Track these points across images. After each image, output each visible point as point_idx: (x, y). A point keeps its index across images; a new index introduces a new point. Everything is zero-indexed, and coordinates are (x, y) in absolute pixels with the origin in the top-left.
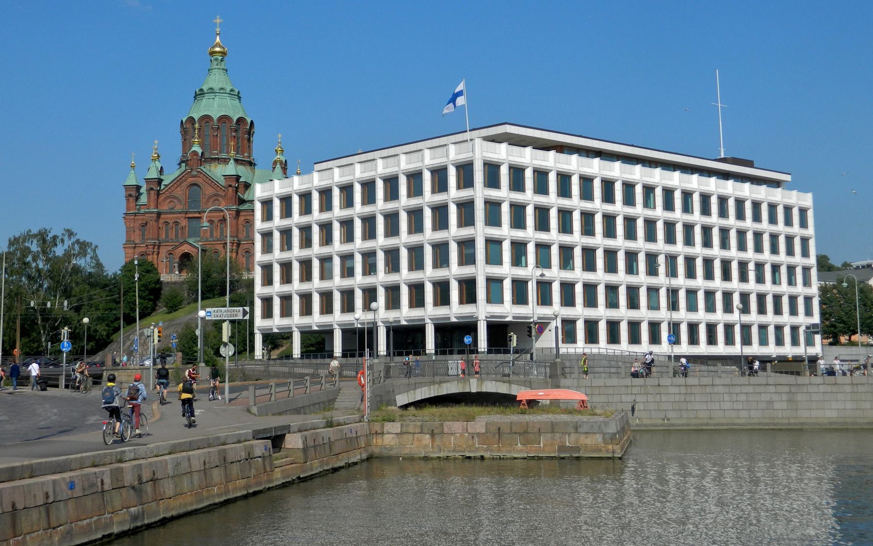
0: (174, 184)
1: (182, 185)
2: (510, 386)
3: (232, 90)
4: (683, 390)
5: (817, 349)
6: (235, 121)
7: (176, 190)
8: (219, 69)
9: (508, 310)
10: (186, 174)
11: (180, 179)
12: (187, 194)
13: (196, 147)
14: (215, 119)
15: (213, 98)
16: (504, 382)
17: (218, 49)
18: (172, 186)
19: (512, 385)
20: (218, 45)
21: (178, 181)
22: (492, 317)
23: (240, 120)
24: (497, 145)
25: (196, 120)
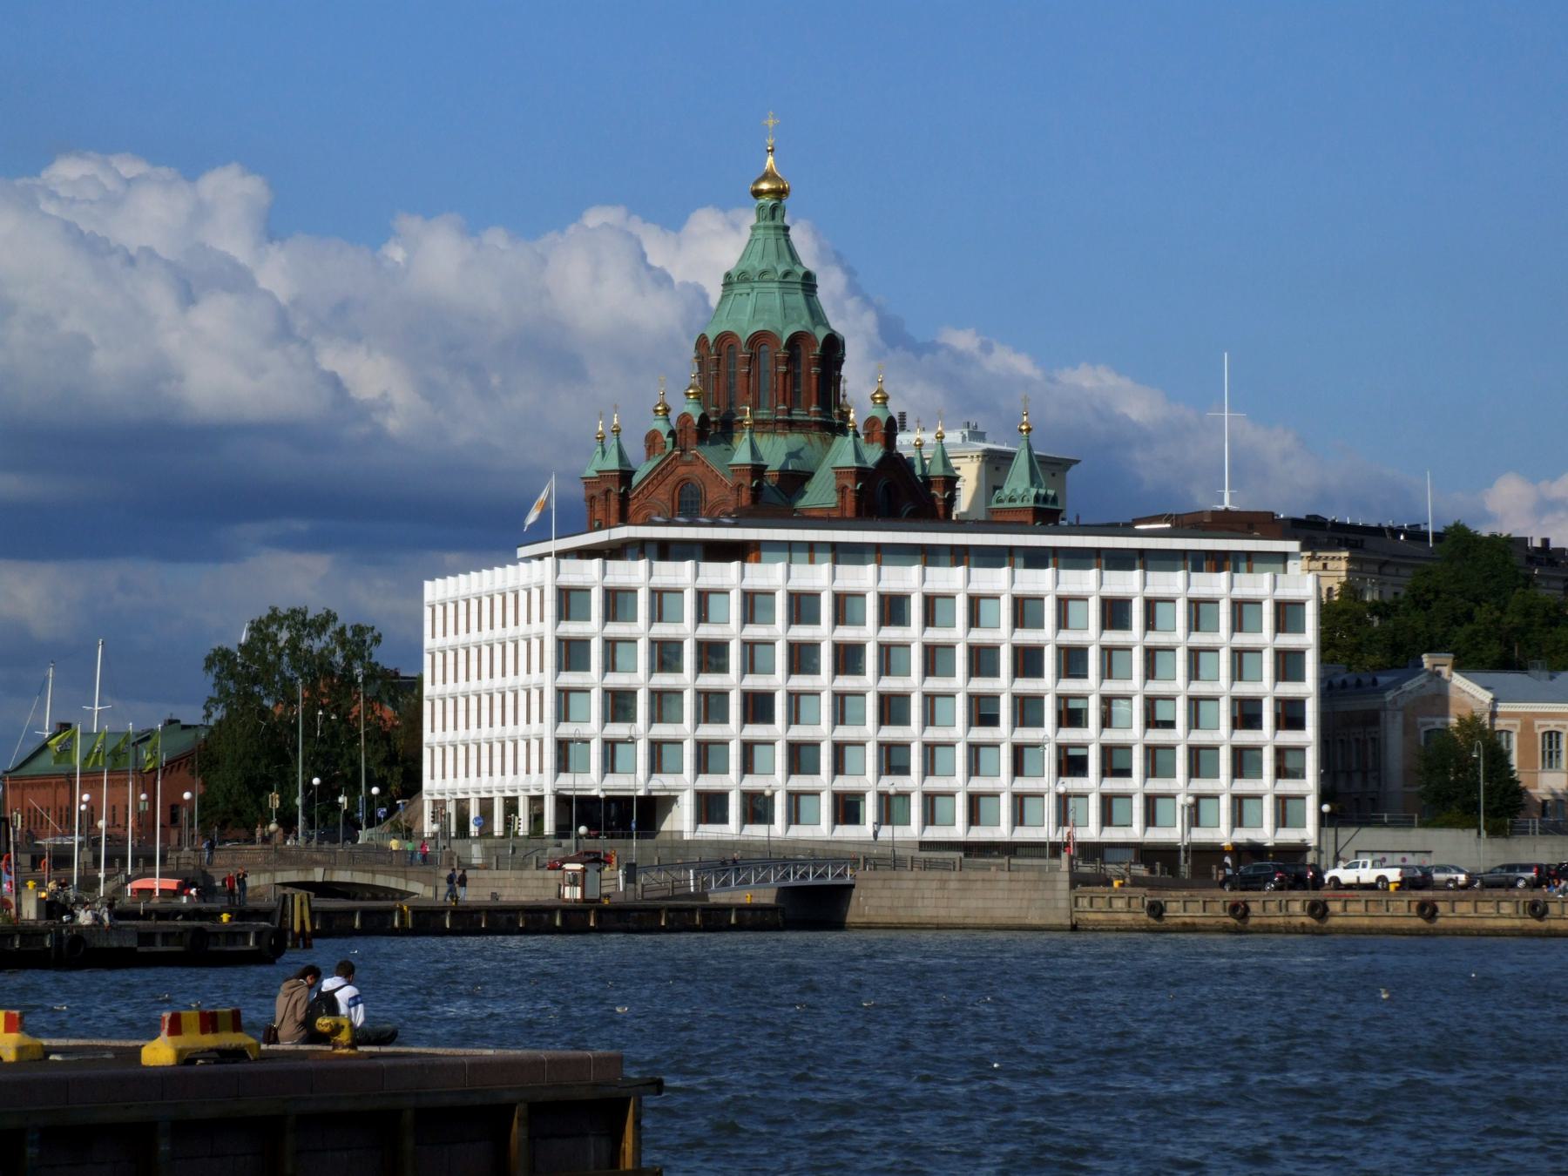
0: (653, 479)
1: (667, 481)
2: (374, 877)
3: (786, 274)
4: (540, 883)
5: (1308, 832)
6: (784, 342)
7: (657, 491)
8: (766, 228)
9: (591, 781)
10: (673, 459)
11: (663, 469)
12: (676, 501)
13: (690, 406)
14: (744, 338)
15: (748, 294)
16: (364, 871)
17: (765, 186)
18: (648, 484)
19: (377, 876)
20: (766, 176)
21: (657, 476)
22: (559, 789)
23: (796, 340)
24: (586, 563)
25: (711, 342)
